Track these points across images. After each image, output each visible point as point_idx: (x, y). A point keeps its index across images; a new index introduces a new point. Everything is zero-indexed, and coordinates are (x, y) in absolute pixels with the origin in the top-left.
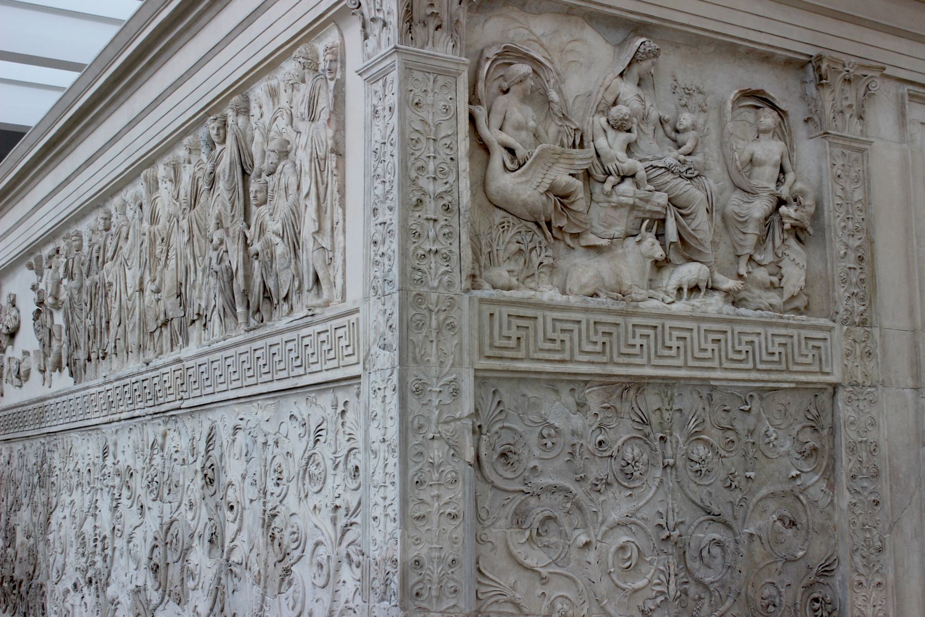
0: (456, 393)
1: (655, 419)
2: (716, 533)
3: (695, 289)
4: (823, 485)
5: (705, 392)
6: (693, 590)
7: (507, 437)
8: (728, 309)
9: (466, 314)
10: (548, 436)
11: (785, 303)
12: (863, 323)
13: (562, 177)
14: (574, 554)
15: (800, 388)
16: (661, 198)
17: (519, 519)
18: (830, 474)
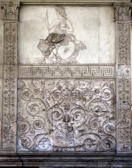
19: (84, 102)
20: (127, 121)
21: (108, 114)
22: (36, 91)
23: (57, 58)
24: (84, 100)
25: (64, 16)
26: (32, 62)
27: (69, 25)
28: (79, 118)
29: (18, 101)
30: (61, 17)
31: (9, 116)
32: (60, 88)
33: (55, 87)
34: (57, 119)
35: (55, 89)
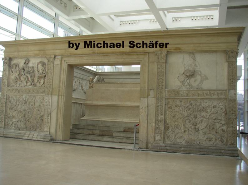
0: (5, 96)
9: (6, 89)
11: (42, 85)
19: (206, 114)
20: (234, 126)
21: (221, 122)
22: (177, 106)
23: (189, 86)
24: (207, 112)
25: (194, 59)
26: (174, 88)
27: (197, 64)
28: (203, 123)
29: (165, 112)
30: (192, 60)
31: (159, 121)
33: (188, 104)
34: (189, 124)
35: (188, 105)
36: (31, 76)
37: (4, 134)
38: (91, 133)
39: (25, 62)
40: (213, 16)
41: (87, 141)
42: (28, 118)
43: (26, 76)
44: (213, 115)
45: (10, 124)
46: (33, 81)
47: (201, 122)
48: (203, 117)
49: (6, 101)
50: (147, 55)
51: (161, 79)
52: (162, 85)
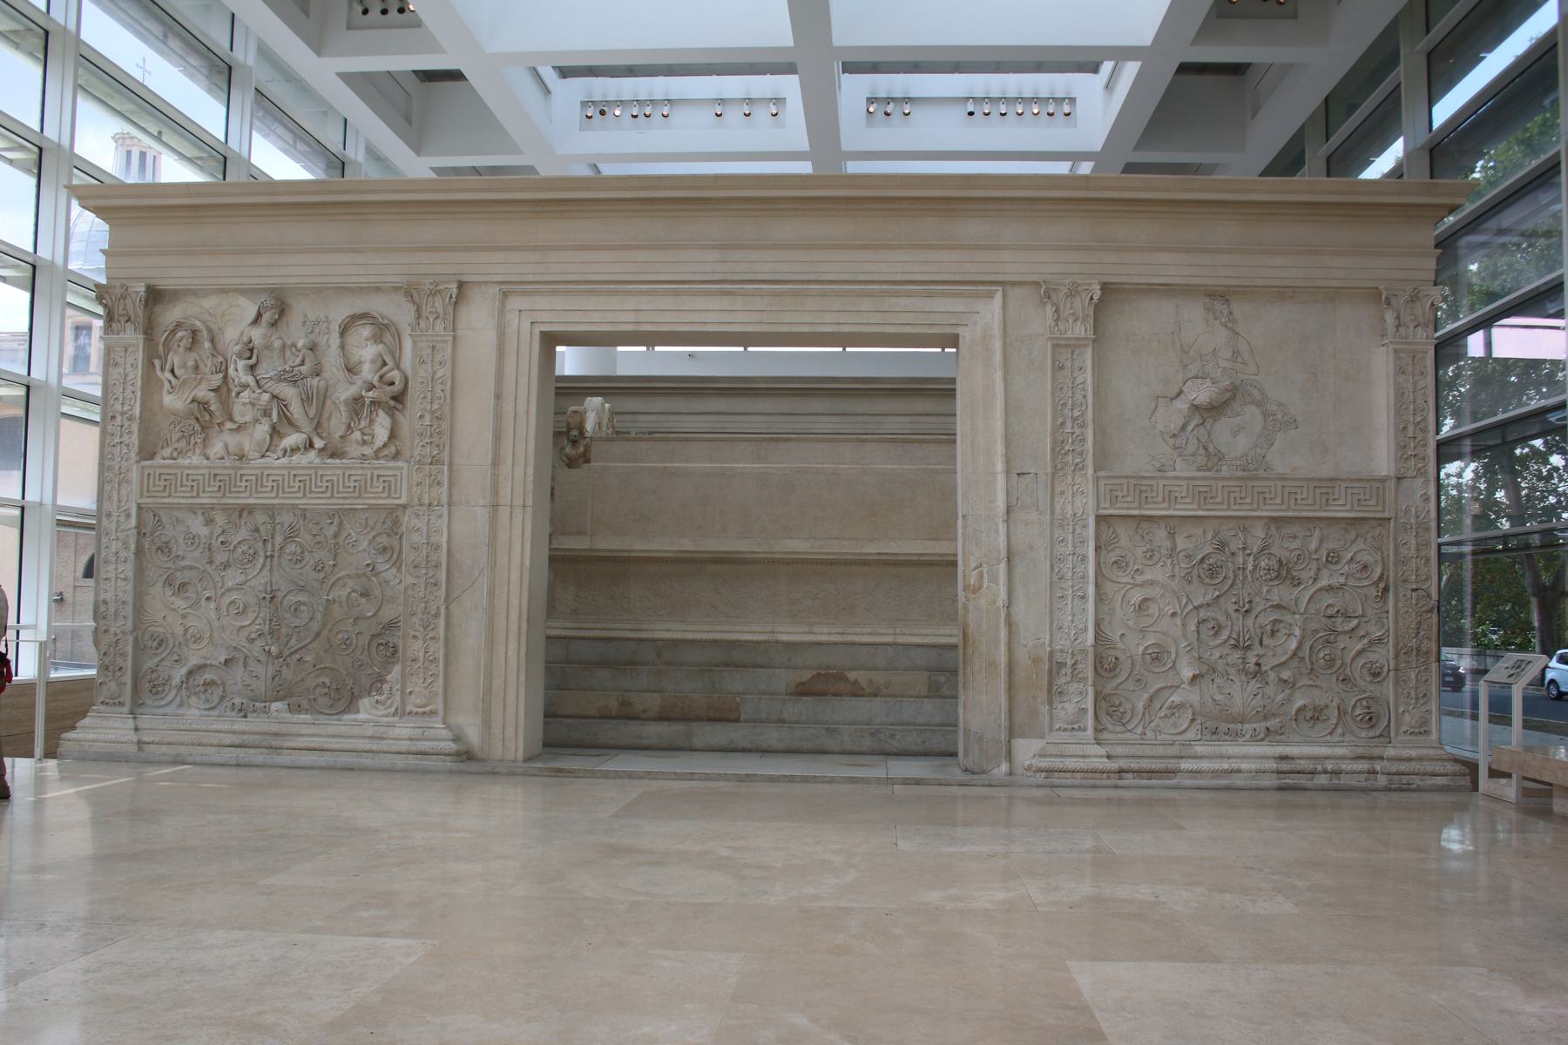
0: (128, 516)
1: (262, 529)
2: (302, 598)
3: (298, 449)
4: (394, 570)
5: (298, 513)
6: (284, 630)
7: (164, 539)
8: (318, 460)
9: (134, 475)
10: (193, 539)
11: (377, 452)
12: (435, 461)
13: (202, 392)
14: (203, 602)
15: (371, 508)
16: (266, 397)
17: (169, 583)
18: (398, 564)
23: (1208, 456)
32: (1222, 546)
35: (1208, 549)
36: (306, 399)
37: (146, 739)
38: (614, 705)
39: (259, 315)
40: (1072, 100)
41: (805, 756)
42: (293, 642)
43: (274, 397)
44: (1329, 599)
45: (176, 680)
46: (318, 427)
47: (1273, 633)
48: (1278, 607)
49: (138, 543)
50: (999, 294)
51: (1074, 420)
52: (1081, 454)
